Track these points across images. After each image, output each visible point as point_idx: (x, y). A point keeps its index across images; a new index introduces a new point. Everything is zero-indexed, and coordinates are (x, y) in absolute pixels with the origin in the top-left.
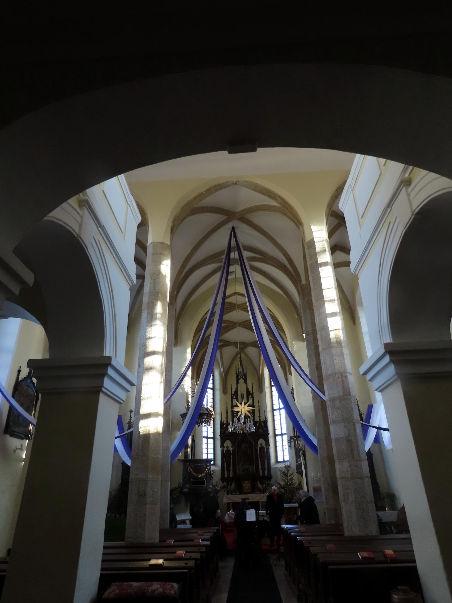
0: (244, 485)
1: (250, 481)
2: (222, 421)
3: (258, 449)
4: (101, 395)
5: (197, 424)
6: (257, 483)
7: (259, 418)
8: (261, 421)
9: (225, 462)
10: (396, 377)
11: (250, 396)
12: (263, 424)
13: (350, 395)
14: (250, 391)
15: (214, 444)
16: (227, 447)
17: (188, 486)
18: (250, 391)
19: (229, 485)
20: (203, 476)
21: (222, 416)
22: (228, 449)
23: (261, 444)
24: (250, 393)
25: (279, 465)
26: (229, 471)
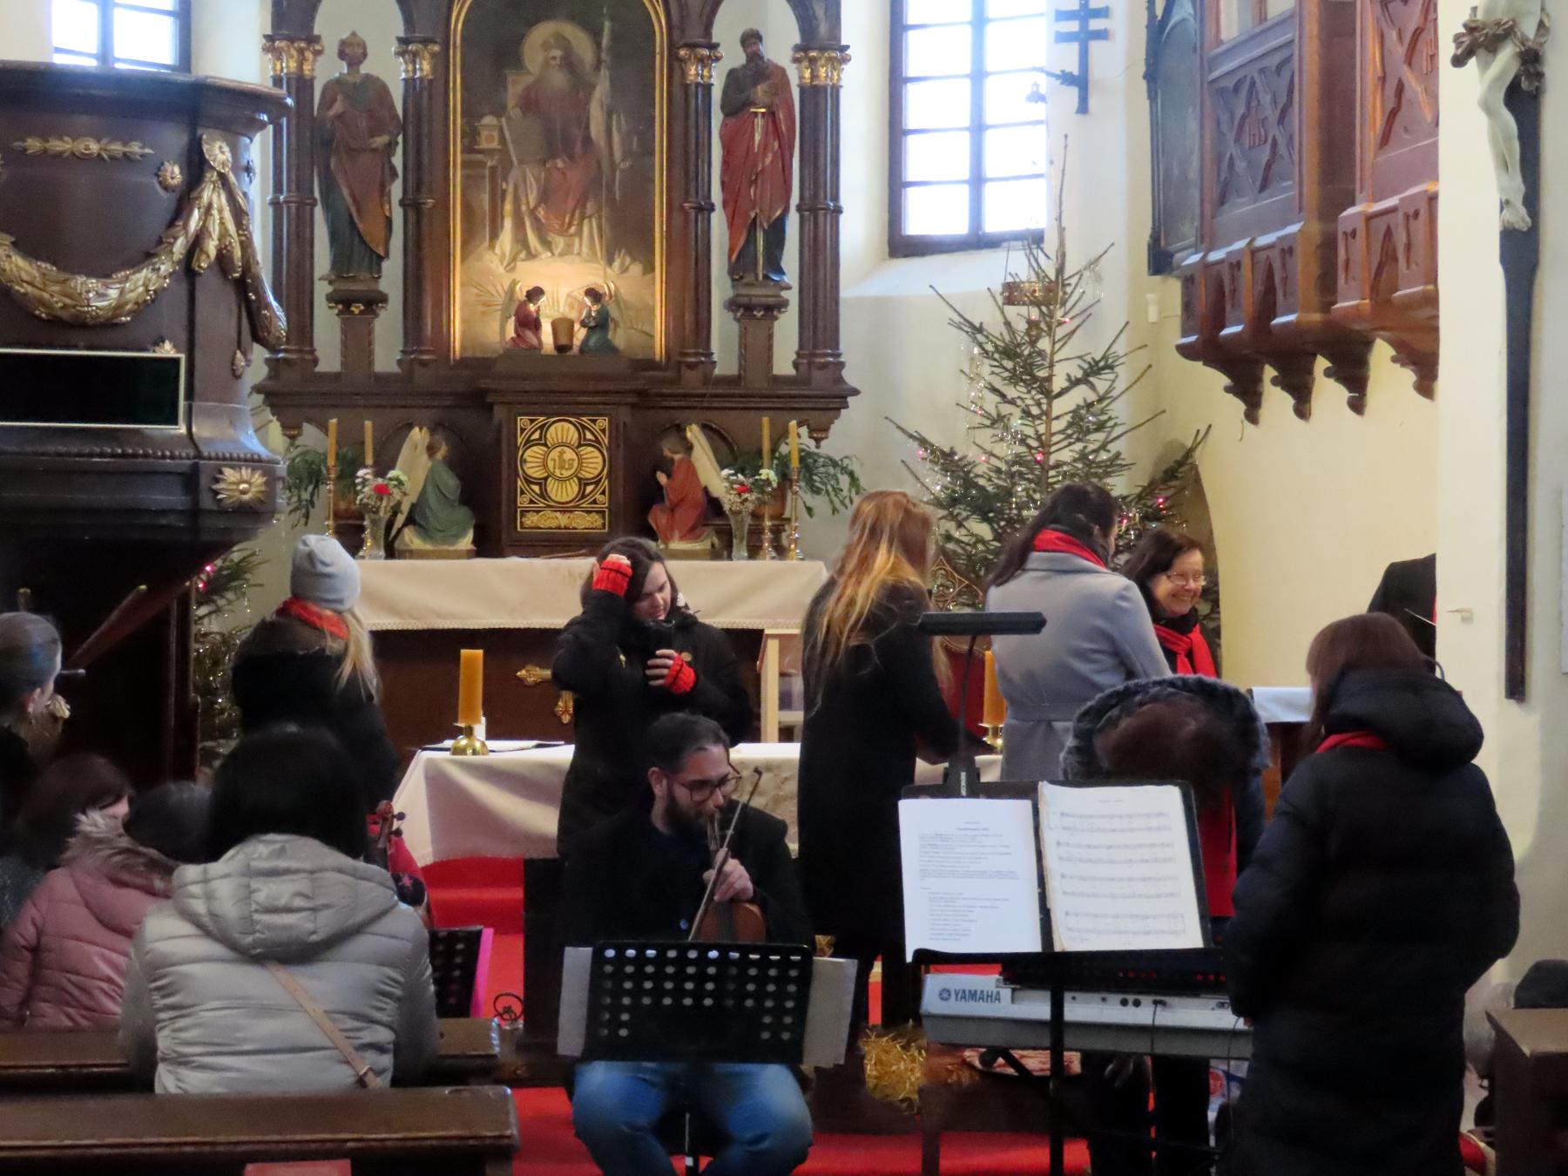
0: (532, 461)
1: (603, 422)
3: (708, 88)
6: (689, 448)
16: (352, 51)
19: (369, 460)
20: (143, 308)
22: (365, 69)
23: (751, 39)
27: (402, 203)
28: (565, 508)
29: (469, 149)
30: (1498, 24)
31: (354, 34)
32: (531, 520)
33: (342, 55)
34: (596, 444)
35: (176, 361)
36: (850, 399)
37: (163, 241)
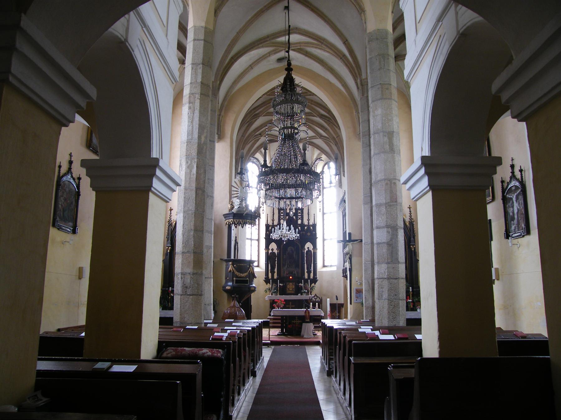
2: (267, 223)
4: (151, 194)
5: (240, 225)
7: (307, 221)
8: (310, 224)
9: (269, 264)
10: (428, 188)
12: (311, 228)
13: (396, 202)
16: (272, 250)
17: (230, 284)
23: (308, 248)
25: (325, 269)
26: (273, 273)
28: (291, 291)
29: (283, 258)
32: (288, 292)
34: (294, 285)
37: (247, 271)
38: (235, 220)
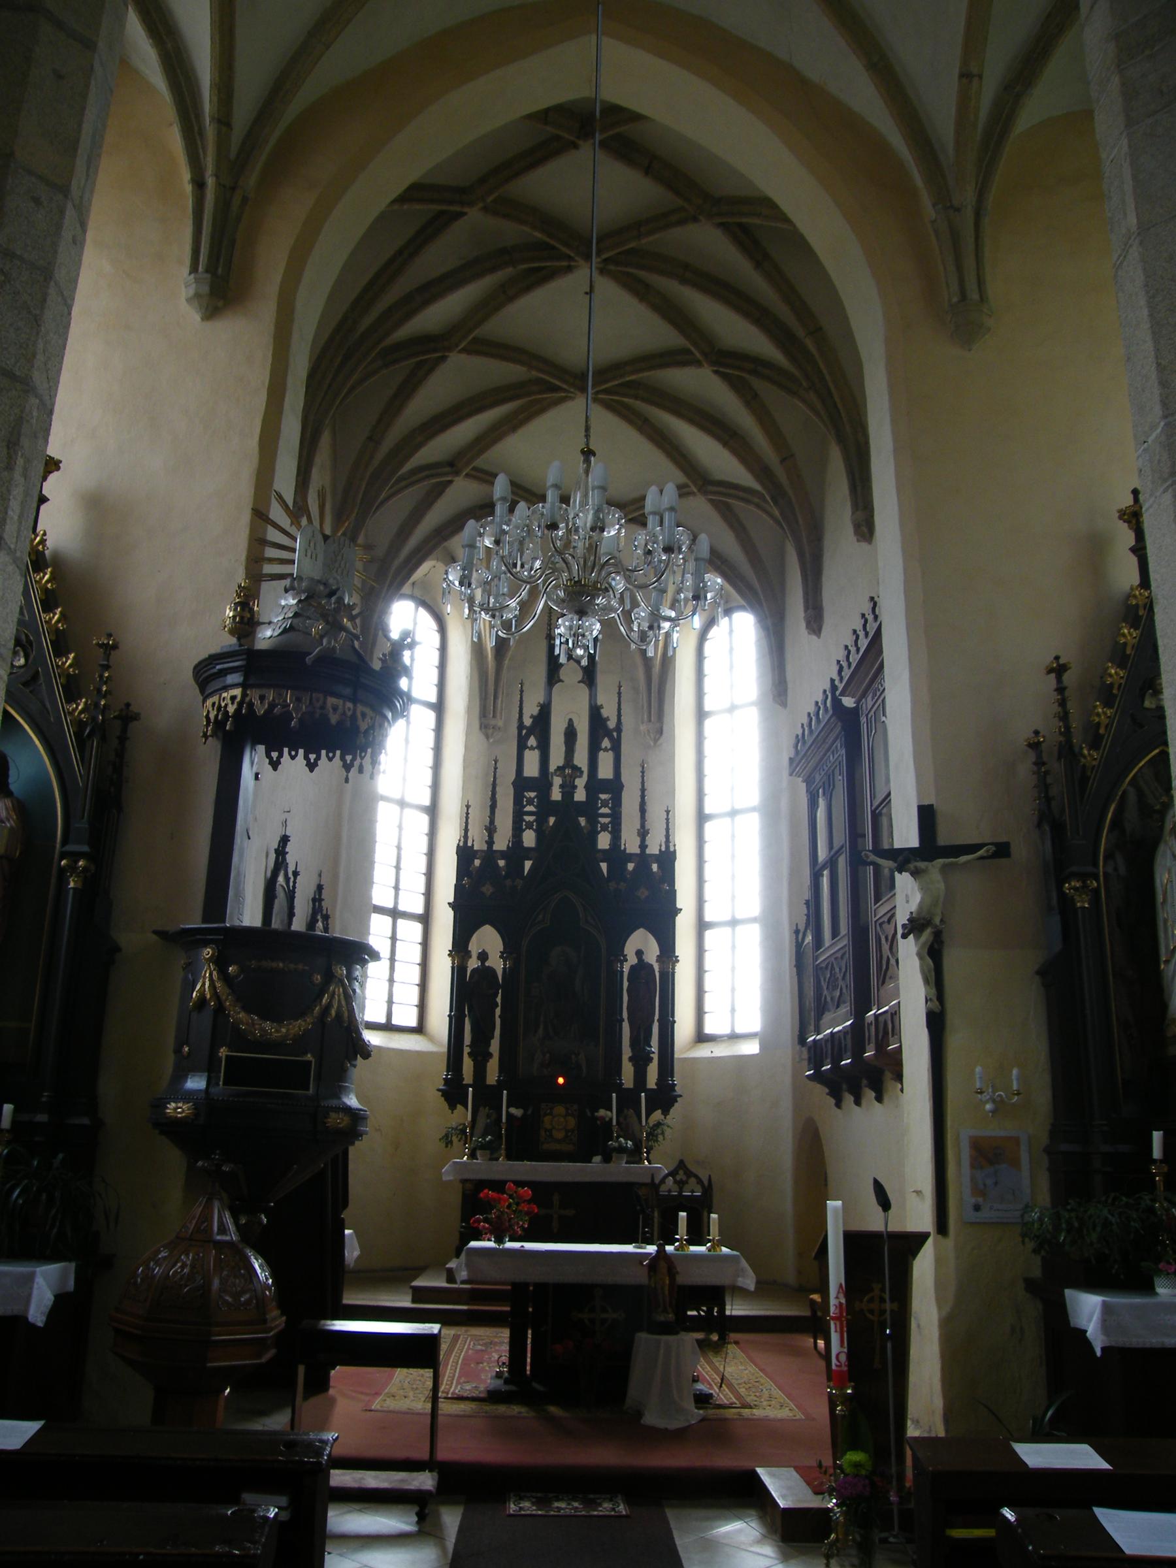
2: (466, 842)
3: (622, 972)
5: (301, 752)
7: (638, 841)
9: (467, 1019)
11: (606, 743)
12: (655, 867)
14: (608, 719)
15: (425, 944)
16: (483, 956)
17: (196, 1083)
18: (608, 719)
21: (467, 818)
23: (639, 953)
24: (606, 726)
25: (705, 1052)
26: (481, 1057)
27: (500, 1017)
30: (924, 919)
31: (484, 950)
32: (545, 1146)
33: (479, 958)
35: (310, 1062)
36: (678, 1099)
38: (254, 695)
